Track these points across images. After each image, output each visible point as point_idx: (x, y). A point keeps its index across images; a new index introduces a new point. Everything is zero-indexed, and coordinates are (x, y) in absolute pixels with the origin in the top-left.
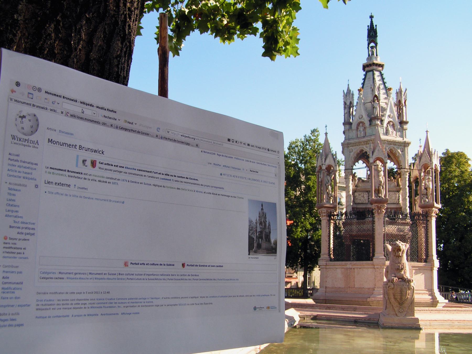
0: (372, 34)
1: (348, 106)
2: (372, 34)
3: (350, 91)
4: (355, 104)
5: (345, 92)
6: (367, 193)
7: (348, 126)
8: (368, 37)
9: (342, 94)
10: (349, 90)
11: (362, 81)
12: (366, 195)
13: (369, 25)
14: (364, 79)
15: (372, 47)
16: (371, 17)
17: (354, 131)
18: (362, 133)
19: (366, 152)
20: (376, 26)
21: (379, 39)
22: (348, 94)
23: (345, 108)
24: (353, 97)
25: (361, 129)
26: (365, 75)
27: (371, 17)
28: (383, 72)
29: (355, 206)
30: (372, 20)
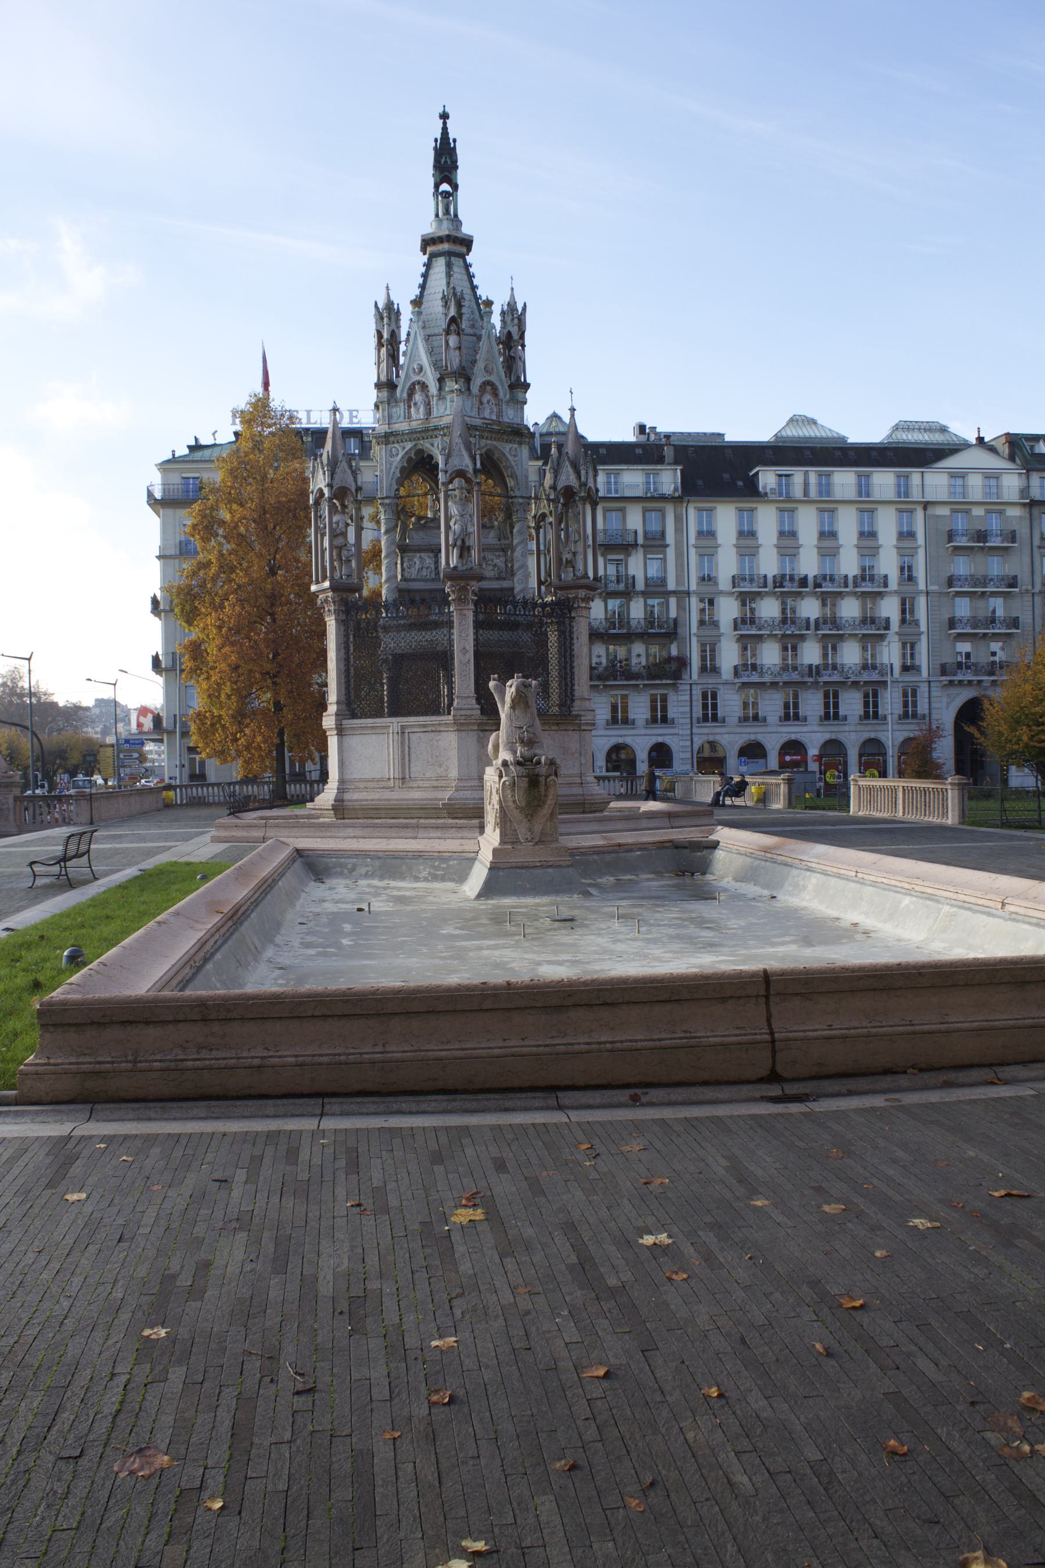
0: (445, 161)
1: (389, 344)
2: (445, 161)
3: (393, 303)
4: (403, 337)
5: (381, 306)
6: (431, 555)
7: (385, 394)
8: (435, 167)
9: (373, 310)
10: (389, 305)
13: (439, 137)
14: (425, 276)
15: (446, 195)
16: (444, 116)
17: (402, 405)
18: (422, 409)
19: (431, 457)
20: (455, 141)
21: (462, 176)
22: (388, 313)
23: (380, 345)
24: (398, 320)
25: (418, 397)
26: (428, 266)
27: (444, 116)
29: (404, 585)
30: (445, 123)
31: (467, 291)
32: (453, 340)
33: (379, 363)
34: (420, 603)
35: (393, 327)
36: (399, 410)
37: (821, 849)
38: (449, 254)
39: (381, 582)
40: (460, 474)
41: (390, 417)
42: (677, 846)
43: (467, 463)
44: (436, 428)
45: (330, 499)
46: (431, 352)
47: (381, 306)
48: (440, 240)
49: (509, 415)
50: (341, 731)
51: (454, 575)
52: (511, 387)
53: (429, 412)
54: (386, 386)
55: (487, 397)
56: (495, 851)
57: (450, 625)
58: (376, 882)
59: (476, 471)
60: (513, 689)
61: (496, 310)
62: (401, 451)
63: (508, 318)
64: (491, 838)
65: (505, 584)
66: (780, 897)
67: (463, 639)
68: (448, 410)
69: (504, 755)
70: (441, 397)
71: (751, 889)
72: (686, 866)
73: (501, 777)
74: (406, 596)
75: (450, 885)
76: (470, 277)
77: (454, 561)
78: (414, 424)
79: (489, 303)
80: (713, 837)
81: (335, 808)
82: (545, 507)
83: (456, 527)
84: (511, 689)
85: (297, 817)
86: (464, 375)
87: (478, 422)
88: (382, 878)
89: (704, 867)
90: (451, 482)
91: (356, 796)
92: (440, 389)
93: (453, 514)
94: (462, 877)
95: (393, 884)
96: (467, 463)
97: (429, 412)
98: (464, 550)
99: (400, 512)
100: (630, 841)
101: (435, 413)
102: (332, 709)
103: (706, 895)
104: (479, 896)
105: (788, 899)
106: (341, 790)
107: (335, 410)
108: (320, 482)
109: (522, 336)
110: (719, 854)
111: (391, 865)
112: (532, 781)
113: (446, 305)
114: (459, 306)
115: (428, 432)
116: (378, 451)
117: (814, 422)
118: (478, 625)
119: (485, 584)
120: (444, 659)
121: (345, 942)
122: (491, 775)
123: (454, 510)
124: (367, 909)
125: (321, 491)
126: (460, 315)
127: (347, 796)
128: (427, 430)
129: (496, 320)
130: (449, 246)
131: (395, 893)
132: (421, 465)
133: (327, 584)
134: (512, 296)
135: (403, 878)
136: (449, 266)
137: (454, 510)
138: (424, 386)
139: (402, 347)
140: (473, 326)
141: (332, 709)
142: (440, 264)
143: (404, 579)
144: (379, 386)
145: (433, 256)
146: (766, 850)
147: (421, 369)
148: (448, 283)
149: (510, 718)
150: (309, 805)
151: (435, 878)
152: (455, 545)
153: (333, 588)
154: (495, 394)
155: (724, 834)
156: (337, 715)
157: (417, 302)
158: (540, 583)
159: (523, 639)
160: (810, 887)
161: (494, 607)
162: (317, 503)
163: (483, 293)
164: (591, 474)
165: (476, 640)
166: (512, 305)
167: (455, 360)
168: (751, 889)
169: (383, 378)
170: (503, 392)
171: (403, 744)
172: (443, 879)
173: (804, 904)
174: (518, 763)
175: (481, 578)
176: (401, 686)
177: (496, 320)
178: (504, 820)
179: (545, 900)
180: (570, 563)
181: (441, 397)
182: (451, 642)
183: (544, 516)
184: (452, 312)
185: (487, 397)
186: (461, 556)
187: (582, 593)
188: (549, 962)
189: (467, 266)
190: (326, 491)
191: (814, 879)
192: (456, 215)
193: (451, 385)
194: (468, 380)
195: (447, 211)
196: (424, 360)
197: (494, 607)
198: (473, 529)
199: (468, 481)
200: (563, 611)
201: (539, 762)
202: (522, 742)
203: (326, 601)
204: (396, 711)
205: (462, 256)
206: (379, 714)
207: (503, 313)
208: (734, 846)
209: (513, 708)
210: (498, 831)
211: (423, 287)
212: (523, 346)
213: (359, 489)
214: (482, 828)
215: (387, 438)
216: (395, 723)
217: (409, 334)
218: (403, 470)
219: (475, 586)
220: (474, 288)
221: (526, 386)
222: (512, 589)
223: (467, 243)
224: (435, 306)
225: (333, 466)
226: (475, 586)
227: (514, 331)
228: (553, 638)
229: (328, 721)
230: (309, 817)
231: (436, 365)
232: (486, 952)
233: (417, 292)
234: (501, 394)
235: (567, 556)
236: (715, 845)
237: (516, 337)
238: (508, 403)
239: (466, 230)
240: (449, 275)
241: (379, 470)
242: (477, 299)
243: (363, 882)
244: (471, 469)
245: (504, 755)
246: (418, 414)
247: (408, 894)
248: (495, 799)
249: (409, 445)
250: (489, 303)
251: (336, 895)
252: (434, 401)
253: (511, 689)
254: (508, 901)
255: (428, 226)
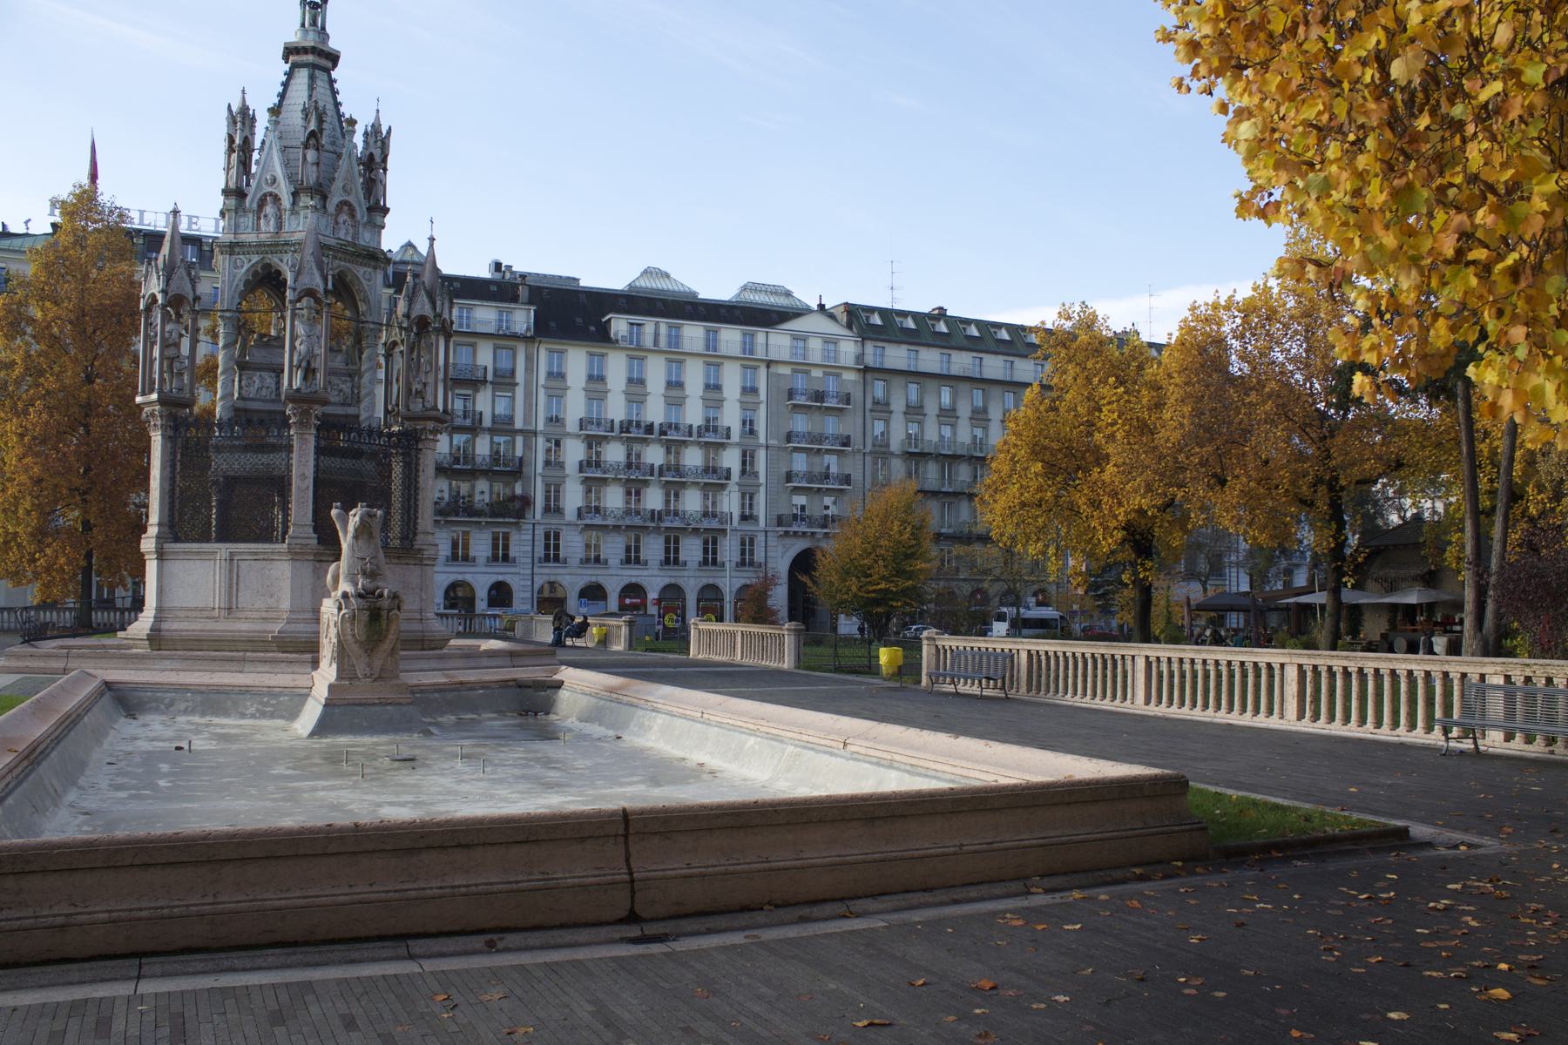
1: (240, 149)
4: (257, 145)
5: (235, 109)
7: (232, 202)
9: (225, 113)
10: (244, 110)
11: (281, 89)
12: (269, 380)
14: (286, 85)
18: (272, 222)
19: (279, 273)
22: (242, 118)
23: (231, 150)
24: (252, 127)
26: (290, 75)
28: (334, 74)
29: (241, 404)
31: (330, 107)
32: (311, 155)
33: (228, 169)
34: (257, 425)
35: (247, 133)
36: (248, 221)
37: (667, 689)
38: (313, 67)
39: (216, 399)
40: (310, 293)
41: (237, 226)
42: (520, 685)
43: (317, 282)
44: (286, 244)
45: (164, 307)
46: (286, 164)
47: (235, 109)
48: (305, 51)
49: (365, 238)
50: (161, 555)
51: (296, 397)
52: (369, 209)
53: (280, 225)
54: (235, 193)
55: (343, 217)
56: (331, 687)
57: (289, 448)
58: (197, 719)
59: (326, 291)
60: (357, 518)
61: (360, 130)
62: (247, 264)
63: (372, 140)
64: (327, 673)
65: (351, 411)
66: (625, 737)
67: (302, 465)
68: (301, 226)
69: (345, 586)
70: (294, 212)
71: (596, 730)
72: (529, 706)
73: (340, 609)
74: (242, 416)
75: (280, 722)
76: (334, 93)
77: (297, 383)
78: (263, 237)
79: (352, 122)
80: (557, 677)
81: (150, 638)
82: (396, 335)
83: (301, 348)
84: (355, 518)
85: (104, 647)
86: (320, 191)
87: (333, 242)
88: (203, 714)
89: (548, 707)
90: (299, 300)
91: (175, 626)
92: (294, 203)
93: (299, 335)
94: (293, 714)
95: (216, 720)
96: (317, 282)
97: (280, 225)
98: (309, 372)
99: (241, 327)
100: (473, 679)
101: (286, 228)
102: (153, 530)
103: (548, 734)
104: (312, 734)
105: (633, 739)
106: (159, 618)
107: (176, 212)
108: (153, 286)
109: (385, 160)
110: (563, 694)
111: (214, 701)
112: (373, 614)
113: (306, 118)
114: (320, 121)
115: (277, 246)
116: (220, 260)
117: (788, 294)
118: (319, 451)
119: (329, 409)
120: (281, 485)
121: (162, 783)
122: (329, 607)
123: (300, 329)
124: (186, 747)
125: (153, 296)
126: (321, 130)
127: (165, 626)
128: (276, 244)
129: (358, 139)
130: (313, 58)
131: (219, 730)
132: (268, 280)
133: (154, 396)
134: (377, 118)
135: (227, 714)
136: (312, 78)
137: (300, 329)
138: (277, 199)
139: (255, 156)
140: (333, 143)
141: (153, 530)
142: (302, 76)
143: (241, 397)
144: (226, 192)
145: (295, 66)
146: (611, 690)
147: (274, 180)
148: (310, 96)
149: (352, 548)
150: (120, 634)
151: (263, 715)
152: (299, 367)
153: (160, 401)
154: (352, 215)
155: (567, 674)
156: (158, 537)
157: (275, 111)
158: (387, 412)
159: (365, 466)
160: (655, 728)
161: (337, 434)
162: (148, 309)
163: (346, 110)
164: (447, 305)
165: (317, 466)
166: (376, 128)
167: (312, 176)
168: (596, 730)
169: (232, 185)
170: (361, 214)
171: (231, 571)
172: (272, 716)
173: (650, 744)
174: (360, 596)
175: (325, 403)
176: (230, 509)
177: (358, 139)
178: (342, 654)
179: (384, 738)
180: (420, 394)
181: (294, 212)
182: (289, 467)
183: (395, 344)
184: (313, 126)
185: (343, 217)
186: (305, 378)
187: (430, 425)
188: (391, 804)
189: (332, 82)
190: (160, 297)
191: (660, 720)
192: (323, 28)
193: (305, 200)
194: (324, 198)
195: (314, 23)
196: (279, 171)
197: (337, 434)
198: (321, 351)
199: (318, 301)
200: (410, 443)
201: (381, 595)
202: (364, 573)
203: (152, 414)
204: (222, 538)
205: (328, 71)
206: (205, 538)
207: (366, 134)
208: (579, 686)
209: (356, 537)
210: (334, 666)
211: (282, 96)
212: (385, 170)
213: (197, 299)
214: (315, 664)
215: (232, 248)
216: (223, 549)
217: (263, 143)
218: (247, 283)
219: (318, 410)
220: (337, 105)
221: (386, 211)
222: (357, 416)
223: (334, 58)
224: (294, 116)
225: (169, 271)
226: (318, 410)
227: (377, 154)
228: (397, 470)
229: (148, 544)
230: (119, 647)
231: (291, 178)
232: (321, 794)
233: (276, 100)
234: (358, 216)
235: (416, 386)
236: (559, 685)
237: (378, 159)
238: (365, 225)
239: (333, 44)
240: (311, 88)
241: (221, 281)
242: (340, 115)
243: (181, 719)
244: (321, 289)
245: (345, 586)
246: (267, 226)
247: (233, 731)
248: (333, 632)
249: (255, 258)
250: (352, 122)
251: (151, 732)
252: (286, 216)
253: (355, 518)
254: (343, 740)
255: (293, 35)
